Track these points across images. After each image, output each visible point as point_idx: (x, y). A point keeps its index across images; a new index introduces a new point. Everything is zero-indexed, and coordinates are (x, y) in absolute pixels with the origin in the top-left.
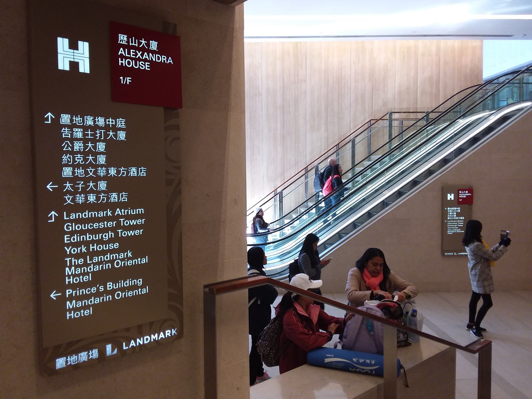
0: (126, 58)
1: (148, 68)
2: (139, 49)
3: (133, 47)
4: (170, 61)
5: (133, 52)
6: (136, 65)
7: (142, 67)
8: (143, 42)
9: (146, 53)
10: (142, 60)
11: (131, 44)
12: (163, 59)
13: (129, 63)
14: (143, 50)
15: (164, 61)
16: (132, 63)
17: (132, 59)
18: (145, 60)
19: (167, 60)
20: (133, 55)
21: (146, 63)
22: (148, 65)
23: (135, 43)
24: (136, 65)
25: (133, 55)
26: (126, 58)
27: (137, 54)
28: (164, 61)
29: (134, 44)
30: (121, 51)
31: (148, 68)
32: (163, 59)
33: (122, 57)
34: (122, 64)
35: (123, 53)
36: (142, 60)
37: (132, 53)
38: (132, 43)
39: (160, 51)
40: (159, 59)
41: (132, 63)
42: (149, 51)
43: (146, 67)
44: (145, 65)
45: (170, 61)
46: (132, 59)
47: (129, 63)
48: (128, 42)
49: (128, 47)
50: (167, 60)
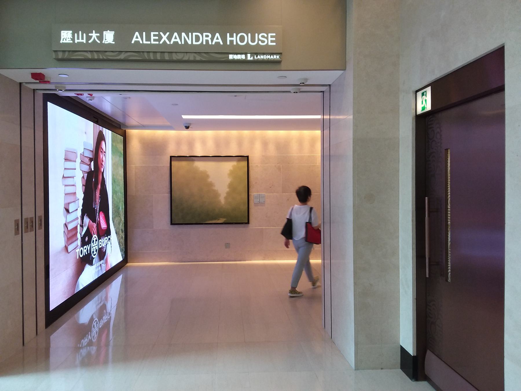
8: (94, 35)
11: (76, 41)
23: (82, 39)
29: (80, 40)
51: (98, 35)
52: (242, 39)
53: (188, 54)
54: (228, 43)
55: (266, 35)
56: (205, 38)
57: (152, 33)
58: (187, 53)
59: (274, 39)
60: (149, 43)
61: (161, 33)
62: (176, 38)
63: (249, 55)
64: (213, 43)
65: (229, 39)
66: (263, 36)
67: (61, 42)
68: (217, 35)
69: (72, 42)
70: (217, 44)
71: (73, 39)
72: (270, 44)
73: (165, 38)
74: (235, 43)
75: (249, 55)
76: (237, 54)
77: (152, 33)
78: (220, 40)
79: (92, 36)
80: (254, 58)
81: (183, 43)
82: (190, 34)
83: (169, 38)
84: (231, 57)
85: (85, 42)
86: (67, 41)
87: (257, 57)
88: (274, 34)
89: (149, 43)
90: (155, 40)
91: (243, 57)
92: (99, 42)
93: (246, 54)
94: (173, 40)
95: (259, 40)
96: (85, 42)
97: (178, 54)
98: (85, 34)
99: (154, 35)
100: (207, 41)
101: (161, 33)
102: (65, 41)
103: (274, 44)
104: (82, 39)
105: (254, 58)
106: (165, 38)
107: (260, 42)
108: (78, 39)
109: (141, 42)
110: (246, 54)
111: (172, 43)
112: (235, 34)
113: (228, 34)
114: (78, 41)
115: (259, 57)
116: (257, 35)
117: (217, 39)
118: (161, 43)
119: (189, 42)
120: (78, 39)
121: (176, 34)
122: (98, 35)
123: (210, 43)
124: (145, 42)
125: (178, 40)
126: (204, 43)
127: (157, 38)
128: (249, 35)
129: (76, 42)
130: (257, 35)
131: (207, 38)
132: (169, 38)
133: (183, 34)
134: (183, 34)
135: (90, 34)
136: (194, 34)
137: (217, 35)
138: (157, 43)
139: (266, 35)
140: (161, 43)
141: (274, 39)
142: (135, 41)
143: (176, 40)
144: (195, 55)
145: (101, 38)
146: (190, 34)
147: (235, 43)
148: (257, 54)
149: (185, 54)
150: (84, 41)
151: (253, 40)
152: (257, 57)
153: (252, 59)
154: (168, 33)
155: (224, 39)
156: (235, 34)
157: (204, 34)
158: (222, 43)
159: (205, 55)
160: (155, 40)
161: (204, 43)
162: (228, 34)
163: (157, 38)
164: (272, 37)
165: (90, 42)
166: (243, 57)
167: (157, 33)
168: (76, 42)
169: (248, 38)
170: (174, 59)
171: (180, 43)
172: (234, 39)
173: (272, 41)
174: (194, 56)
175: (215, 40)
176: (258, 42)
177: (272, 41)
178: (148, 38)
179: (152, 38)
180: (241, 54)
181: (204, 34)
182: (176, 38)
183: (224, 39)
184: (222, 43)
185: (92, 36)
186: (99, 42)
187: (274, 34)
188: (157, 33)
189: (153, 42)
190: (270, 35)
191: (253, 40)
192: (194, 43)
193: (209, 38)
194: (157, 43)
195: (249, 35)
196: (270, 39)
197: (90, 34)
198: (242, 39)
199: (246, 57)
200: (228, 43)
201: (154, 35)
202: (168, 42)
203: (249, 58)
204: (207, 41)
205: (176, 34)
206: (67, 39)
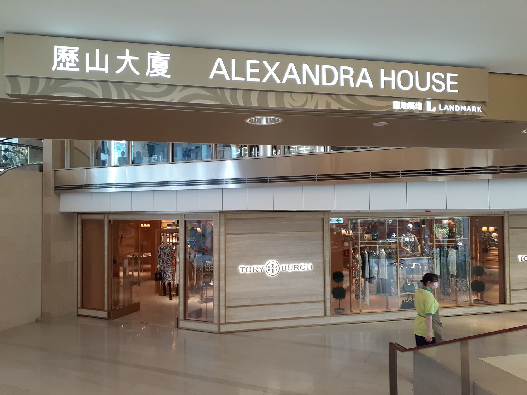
8: (128, 59)
11: (88, 69)
23: (102, 65)
29: (97, 68)
51: (137, 58)
52: (405, 80)
54: (383, 86)
55: (443, 76)
56: (343, 76)
57: (249, 62)
59: (456, 83)
60: (243, 79)
61: (265, 63)
62: (291, 73)
64: (358, 85)
65: (383, 79)
66: (438, 78)
67: (53, 69)
68: (364, 70)
69: (78, 70)
70: (364, 86)
71: (81, 64)
72: (449, 90)
73: (271, 71)
74: (393, 87)
77: (249, 62)
78: (369, 81)
79: (123, 61)
81: (304, 82)
82: (317, 66)
83: (280, 72)
85: (107, 72)
86: (68, 69)
88: (456, 75)
89: (243, 79)
90: (253, 75)
92: (138, 73)
94: (287, 76)
95: (432, 83)
96: (107, 72)
98: (107, 56)
99: (252, 66)
100: (346, 81)
101: (265, 63)
102: (61, 68)
103: (457, 91)
104: (102, 65)
106: (271, 71)
107: (434, 87)
108: (92, 64)
109: (227, 78)
111: (284, 81)
112: (393, 72)
113: (382, 71)
114: (93, 69)
116: (428, 74)
117: (364, 78)
118: (265, 80)
119: (316, 82)
120: (92, 64)
121: (291, 66)
122: (137, 58)
123: (352, 85)
124: (234, 78)
125: (296, 76)
126: (342, 84)
127: (257, 71)
128: (417, 73)
129: (88, 71)
130: (428, 74)
131: (346, 76)
132: (280, 72)
133: (305, 67)
134: (305, 67)
135: (118, 57)
136: (324, 67)
137: (364, 70)
138: (258, 80)
139: (443, 76)
140: (265, 80)
141: (456, 83)
142: (216, 75)
143: (291, 77)
145: (142, 65)
146: (317, 66)
147: (393, 87)
150: (106, 70)
151: (423, 84)
154: (278, 64)
155: (376, 79)
156: (393, 72)
157: (342, 68)
158: (371, 86)
160: (253, 75)
161: (342, 84)
162: (382, 71)
163: (257, 71)
164: (452, 79)
165: (118, 72)
167: (258, 62)
168: (88, 71)
169: (414, 79)
171: (299, 82)
172: (392, 79)
173: (452, 87)
175: (360, 80)
176: (431, 87)
177: (452, 87)
178: (241, 72)
179: (249, 70)
181: (342, 68)
182: (291, 73)
183: (376, 79)
184: (371, 86)
185: (123, 61)
186: (138, 73)
187: (456, 75)
188: (258, 62)
189: (249, 79)
190: (449, 75)
191: (423, 84)
192: (324, 83)
193: (350, 77)
194: (258, 80)
195: (417, 73)
196: (449, 83)
197: (118, 57)
198: (405, 80)
200: (383, 86)
201: (252, 66)
202: (278, 81)
204: (346, 81)
205: (291, 66)
206: (68, 64)
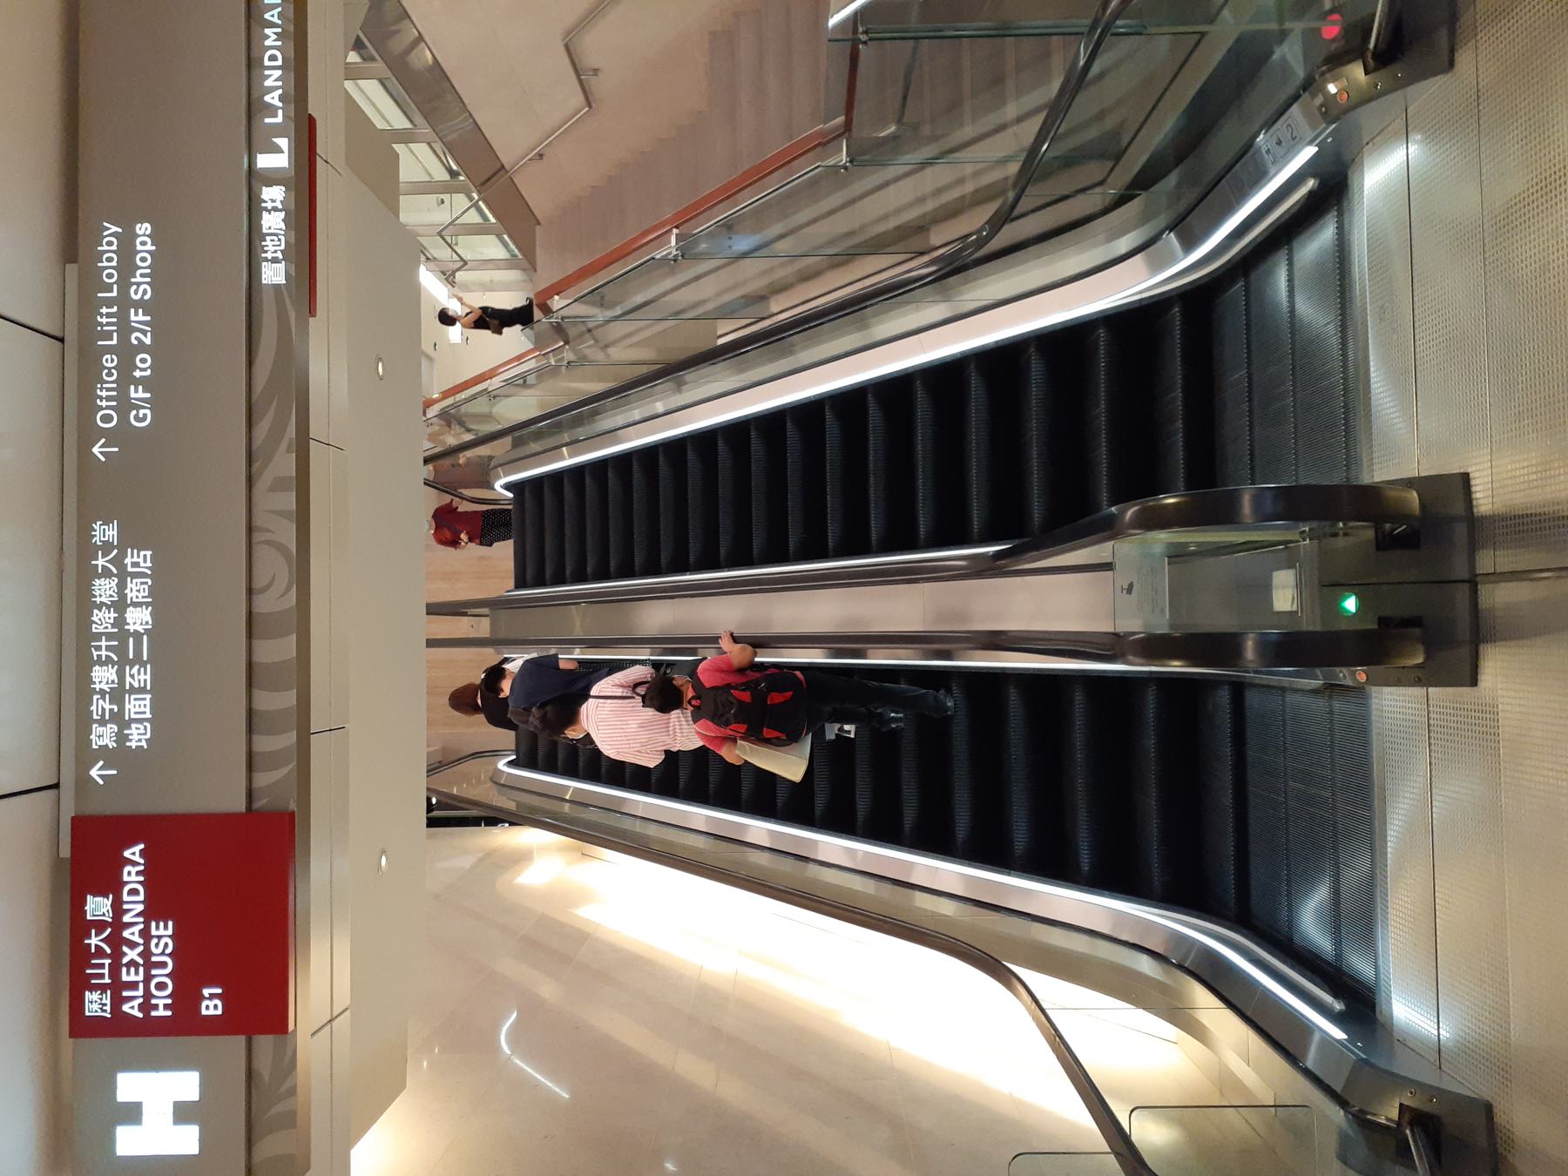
0: (148, 995)
1: (166, 927)
2: (117, 955)
3: (115, 971)
4: (134, 852)
5: (128, 973)
6: (163, 965)
7: (166, 945)
9: (126, 934)
10: (147, 944)
12: (132, 876)
13: (161, 986)
14: (116, 941)
15: (138, 873)
16: (161, 975)
17: (148, 978)
18: (146, 934)
19: (135, 864)
20: (137, 973)
21: (154, 932)
22: (157, 928)
24: (163, 965)
25: (137, 973)
26: (148, 995)
27: (132, 963)
28: (138, 873)
30: (132, 1009)
31: (166, 927)
32: (132, 876)
33: (146, 1006)
34: (166, 1007)
35: (136, 1003)
36: (147, 944)
37: (132, 978)
38: (102, 976)
39: (111, 885)
40: (134, 892)
41: (161, 975)
42: (118, 925)
43: (164, 932)
44: (159, 937)
45: (134, 852)
46: (148, 978)
47: (161, 986)
48: (102, 988)
49: (117, 988)
50: (135, 864)
53: (258, 521)
58: (250, 529)
63: (264, 161)
75: (264, 161)
76: (254, 235)
80: (279, 131)
84: (273, 275)
87: (272, 111)
91: (273, 195)
93: (256, 179)
97: (259, 582)
105: (279, 131)
110: (256, 179)
115: (273, 99)
144: (261, 487)
148: (254, 108)
149: (257, 537)
152: (272, 111)
153: (283, 142)
159: (262, 429)
166: (273, 195)
170: (292, 599)
174: (271, 489)
180: (254, 208)
199: (272, 178)
203: (275, 160)
